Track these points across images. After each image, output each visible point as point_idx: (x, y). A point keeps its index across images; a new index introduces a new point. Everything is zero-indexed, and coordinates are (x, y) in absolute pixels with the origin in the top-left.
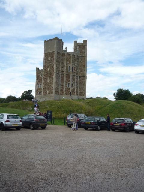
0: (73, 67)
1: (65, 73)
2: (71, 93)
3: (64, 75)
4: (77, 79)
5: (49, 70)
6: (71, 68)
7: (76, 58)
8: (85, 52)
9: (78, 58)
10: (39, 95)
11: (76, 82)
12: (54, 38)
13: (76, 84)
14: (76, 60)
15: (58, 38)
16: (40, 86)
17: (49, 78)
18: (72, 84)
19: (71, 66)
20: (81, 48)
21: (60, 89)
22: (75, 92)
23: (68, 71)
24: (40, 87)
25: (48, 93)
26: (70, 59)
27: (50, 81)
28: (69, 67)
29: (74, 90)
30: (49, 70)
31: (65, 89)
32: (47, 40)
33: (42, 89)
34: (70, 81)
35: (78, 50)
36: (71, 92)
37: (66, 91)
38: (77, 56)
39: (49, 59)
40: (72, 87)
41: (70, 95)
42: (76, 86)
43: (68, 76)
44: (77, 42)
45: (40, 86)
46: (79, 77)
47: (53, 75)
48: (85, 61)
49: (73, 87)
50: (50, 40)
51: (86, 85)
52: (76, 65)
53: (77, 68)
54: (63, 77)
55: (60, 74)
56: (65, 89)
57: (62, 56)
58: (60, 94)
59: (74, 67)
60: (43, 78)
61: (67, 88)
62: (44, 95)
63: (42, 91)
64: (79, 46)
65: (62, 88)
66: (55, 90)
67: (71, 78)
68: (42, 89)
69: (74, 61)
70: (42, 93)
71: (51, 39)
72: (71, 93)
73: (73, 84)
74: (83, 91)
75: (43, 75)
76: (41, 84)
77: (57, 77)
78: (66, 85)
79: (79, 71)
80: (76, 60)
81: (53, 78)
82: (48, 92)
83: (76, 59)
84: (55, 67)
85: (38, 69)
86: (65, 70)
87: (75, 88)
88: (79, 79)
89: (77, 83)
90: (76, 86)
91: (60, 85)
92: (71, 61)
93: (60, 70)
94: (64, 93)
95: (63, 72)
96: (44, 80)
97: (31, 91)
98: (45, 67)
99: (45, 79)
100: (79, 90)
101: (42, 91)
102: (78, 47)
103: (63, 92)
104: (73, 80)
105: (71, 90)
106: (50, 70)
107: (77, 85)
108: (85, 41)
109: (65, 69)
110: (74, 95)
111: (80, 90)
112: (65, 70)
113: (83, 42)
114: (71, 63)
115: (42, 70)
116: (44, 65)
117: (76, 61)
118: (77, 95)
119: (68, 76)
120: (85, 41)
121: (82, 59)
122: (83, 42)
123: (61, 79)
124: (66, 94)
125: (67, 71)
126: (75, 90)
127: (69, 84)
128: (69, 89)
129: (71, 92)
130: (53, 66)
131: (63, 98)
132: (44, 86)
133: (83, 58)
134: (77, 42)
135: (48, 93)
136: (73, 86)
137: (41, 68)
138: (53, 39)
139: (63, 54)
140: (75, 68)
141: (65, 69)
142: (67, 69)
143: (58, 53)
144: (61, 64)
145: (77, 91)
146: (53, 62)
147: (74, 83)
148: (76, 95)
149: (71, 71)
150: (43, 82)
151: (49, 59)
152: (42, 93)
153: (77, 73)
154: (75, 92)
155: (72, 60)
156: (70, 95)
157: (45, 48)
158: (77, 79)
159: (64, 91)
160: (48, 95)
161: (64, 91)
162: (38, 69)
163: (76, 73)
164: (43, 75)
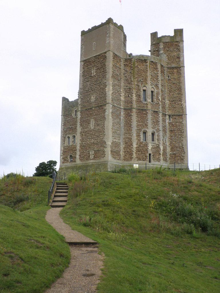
0: (152, 92)
1: (135, 105)
2: (150, 154)
3: (131, 109)
4: (164, 121)
5: (93, 99)
6: (149, 93)
7: (159, 69)
8: (179, 58)
9: (162, 72)
10: (69, 164)
11: (161, 128)
12: (104, 21)
13: (161, 133)
14: (160, 75)
15: (114, 22)
16: (71, 139)
17: (96, 120)
18: (153, 134)
19: (149, 88)
20: (169, 47)
21: (122, 146)
22: (161, 152)
23: (140, 101)
24: (71, 144)
25: (92, 157)
26: (146, 71)
27: (98, 125)
28: (144, 91)
29: (158, 147)
30: (93, 99)
31: (135, 145)
32: (86, 29)
33: (78, 148)
34: (146, 125)
35: (162, 52)
36: (150, 152)
37: (138, 150)
38: (162, 66)
39: (94, 72)
40: (153, 140)
41: (150, 162)
42: (161, 138)
43: (142, 112)
44: (159, 35)
45: (71, 139)
46: (167, 117)
47: (105, 110)
48: (182, 79)
49: (156, 141)
50: (95, 28)
51: (186, 136)
52: (160, 86)
53: (163, 95)
54: (128, 116)
55: (122, 107)
56: (135, 145)
57: (124, 65)
58: (122, 157)
59: (156, 90)
60: (79, 121)
61: (140, 143)
62: (84, 162)
63: (78, 153)
64: (165, 43)
65: (128, 144)
66: (111, 147)
67: (150, 116)
68: (78, 148)
69: (155, 78)
70: (78, 157)
71: (98, 23)
72: (150, 154)
73: (156, 134)
74: (179, 152)
75: (79, 114)
76: (74, 137)
77: (116, 115)
78: (138, 136)
79: (167, 102)
80: (160, 75)
81: (104, 118)
82: (92, 153)
83: (159, 72)
84: (110, 91)
85: (65, 100)
86: (134, 98)
87: (161, 142)
88: (167, 121)
89: (164, 131)
90: (161, 138)
91: (122, 137)
92: (147, 76)
93: (122, 98)
94: (134, 155)
95: (129, 102)
96: (81, 125)
97: (55, 163)
98: (84, 92)
99: (85, 122)
100: (168, 149)
101: (78, 153)
102: (161, 46)
103: (131, 154)
104: (156, 122)
105: (150, 147)
106: (96, 99)
107: (163, 137)
108: (179, 32)
109: (134, 95)
110: (159, 160)
111: (172, 149)
112: (134, 98)
113: (172, 34)
114: (149, 82)
115: (76, 101)
116: (80, 89)
117: (160, 79)
118: (165, 160)
119: (142, 112)
120: (179, 32)
121: (173, 73)
122: (172, 34)
123: (126, 121)
124: (139, 159)
125: (139, 101)
126: (162, 148)
127: (145, 133)
128: (146, 145)
129: (150, 152)
130: (104, 89)
131: (135, 165)
132: (82, 140)
133: (175, 71)
134: (159, 35)
135: (92, 157)
136: (156, 137)
137: (73, 96)
138: (102, 25)
139: (126, 60)
140: (158, 94)
141: (134, 95)
142: (139, 96)
143: (115, 56)
144: (122, 84)
145: (165, 150)
146: (104, 77)
147: (158, 130)
148: (164, 160)
149: (149, 100)
150: (79, 129)
151: (94, 72)
152: (78, 157)
153: (164, 107)
154: (161, 152)
155: (149, 74)
156: (150, 162)
157: (81, 48)
158: (164, 121)
159: (134, 150)
160: (92, 161)
161: (134, 150)
162: (65, 100)
163: (161, 107)
164: (79, 116)
